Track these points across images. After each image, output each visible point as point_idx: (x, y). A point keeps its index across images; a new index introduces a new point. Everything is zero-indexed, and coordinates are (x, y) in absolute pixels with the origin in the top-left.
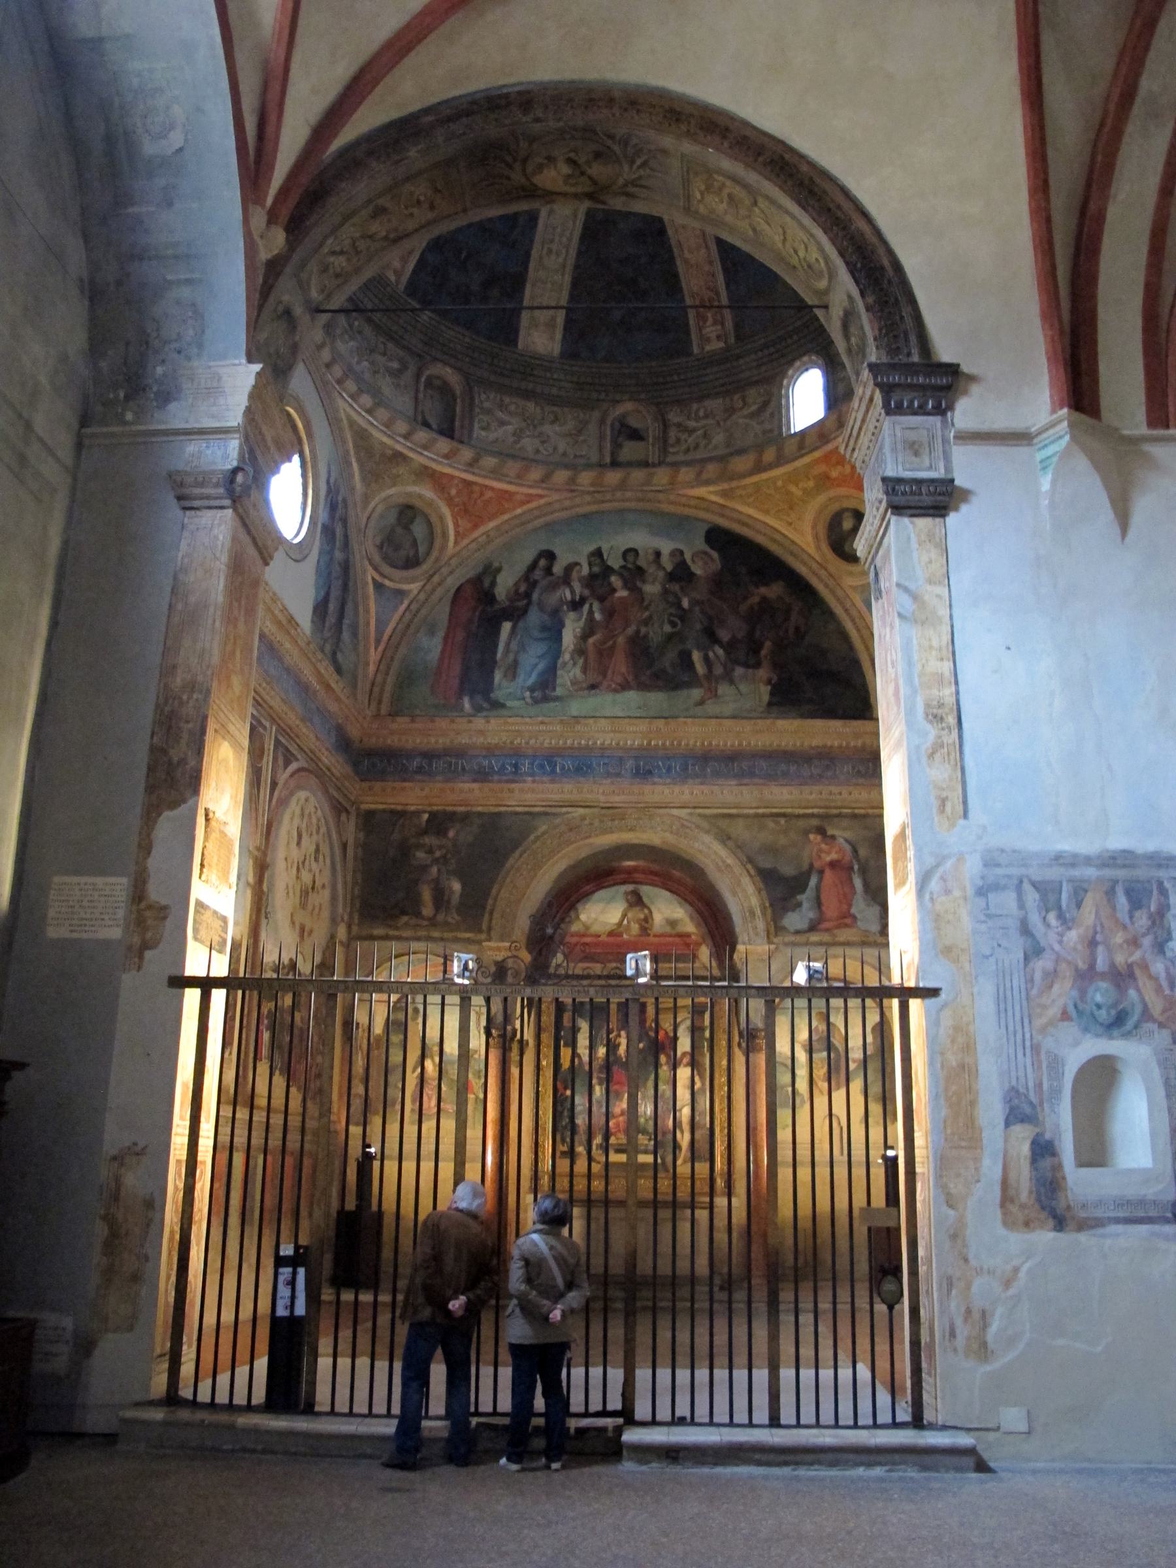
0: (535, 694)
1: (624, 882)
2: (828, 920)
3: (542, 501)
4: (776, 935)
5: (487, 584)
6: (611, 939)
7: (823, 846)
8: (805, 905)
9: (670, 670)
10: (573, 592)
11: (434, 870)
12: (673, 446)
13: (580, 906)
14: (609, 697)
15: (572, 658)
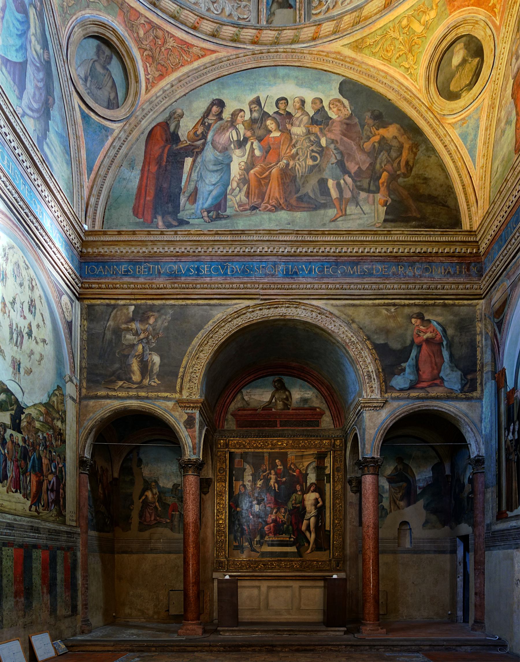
0: (211, 214)
2: (423, 382)
3: (214, 56)
4: (386, 392)
5: (172, 128)
7: (421, 327)
8: (408, 370)
9: (311, 195)
10: (238, 134)
11: (140, 347)
12: (316, 8)
14: (266, 216)
15: (238, 186)
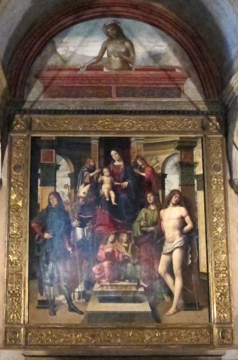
1: (103, 15)
6: (91, 73)
13: (56, 39)
